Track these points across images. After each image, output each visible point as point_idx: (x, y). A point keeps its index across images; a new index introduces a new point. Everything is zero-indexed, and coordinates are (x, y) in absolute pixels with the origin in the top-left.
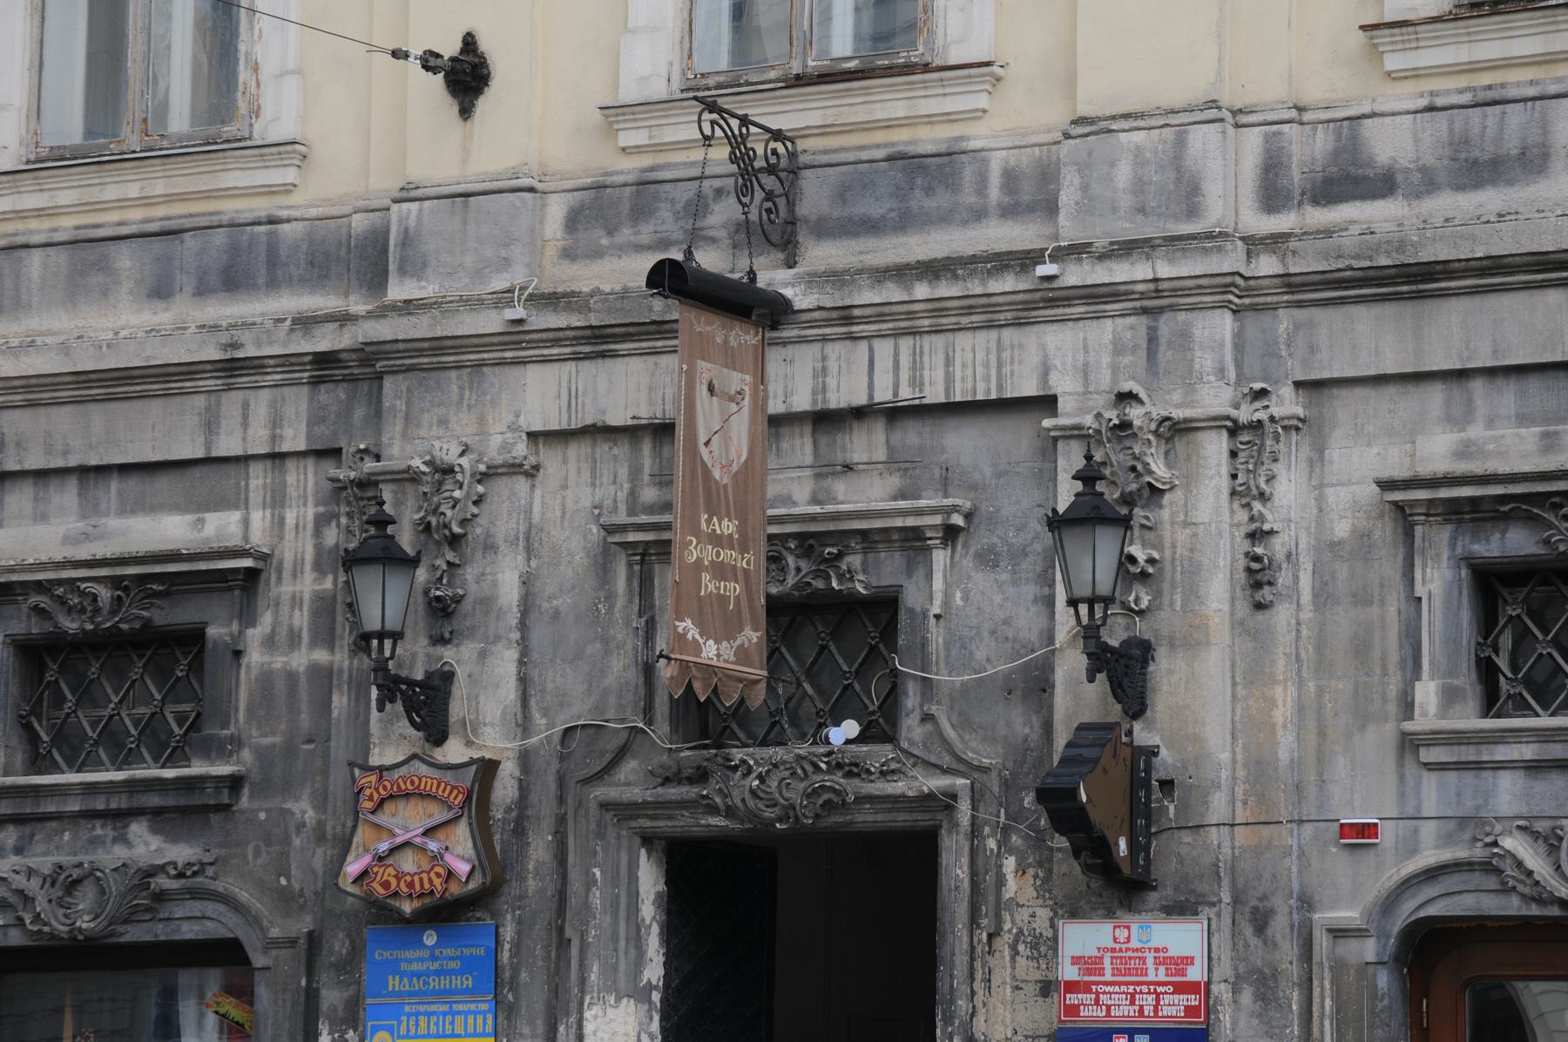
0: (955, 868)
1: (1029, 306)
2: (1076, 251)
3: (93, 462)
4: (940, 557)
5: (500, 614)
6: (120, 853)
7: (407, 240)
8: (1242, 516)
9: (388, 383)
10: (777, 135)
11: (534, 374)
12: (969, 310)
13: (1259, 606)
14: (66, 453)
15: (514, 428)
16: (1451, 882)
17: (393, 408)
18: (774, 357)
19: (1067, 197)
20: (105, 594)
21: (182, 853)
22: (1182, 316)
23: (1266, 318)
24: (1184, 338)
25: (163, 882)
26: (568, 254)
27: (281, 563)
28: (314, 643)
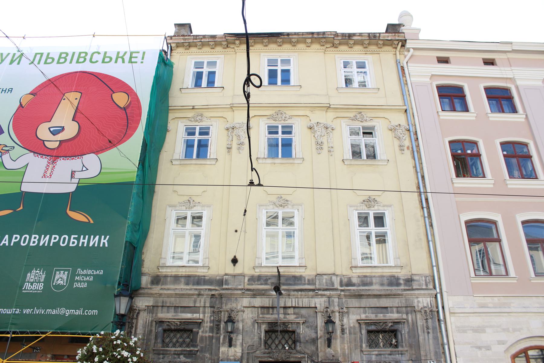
2: (319, 290)
3: (177, 305)
4: (301, 326)
5: (240, 330)
6: (179, 359)
8: (340, 323)
9: (223, 299)
12: (305, 296)
13: (343, 334)
14: (173, 304)
17: (224, 302)
19: (317, 283)
22: (333, 298)
23: (342, 299)
24: (333, 301)
26: (248, 284)
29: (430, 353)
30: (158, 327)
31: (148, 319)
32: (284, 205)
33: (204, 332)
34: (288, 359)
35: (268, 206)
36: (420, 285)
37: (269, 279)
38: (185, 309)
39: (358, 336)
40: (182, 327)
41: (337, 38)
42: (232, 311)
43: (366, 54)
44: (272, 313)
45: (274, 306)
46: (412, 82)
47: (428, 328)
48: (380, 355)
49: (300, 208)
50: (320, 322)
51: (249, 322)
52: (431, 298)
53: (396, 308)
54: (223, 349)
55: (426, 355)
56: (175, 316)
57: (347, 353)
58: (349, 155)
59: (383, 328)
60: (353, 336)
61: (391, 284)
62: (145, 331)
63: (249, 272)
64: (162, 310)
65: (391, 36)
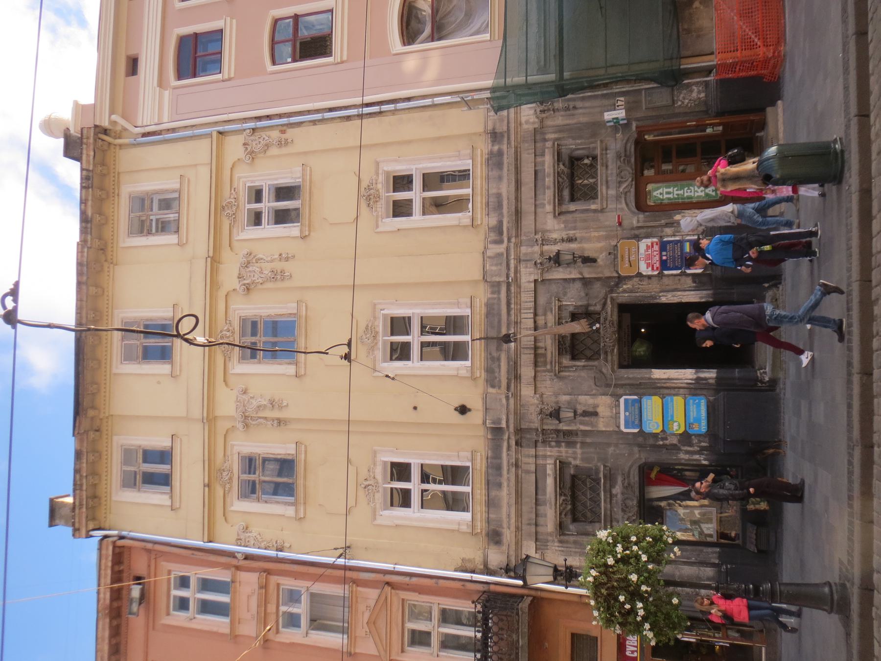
4: (564, 303)
7: (493, 423)
8: (559, 244)
9: (522, 427)
11: (523, 393)
12: (517, 297)
13: (576, 239)
14: (532, 508)
15: (533, 397)
16: (628, 201)
19: (497, 279)
20: (563, 498)
21: (620, 479)
22: (521, 255)
24: (526, 254)
25: (626, 484)
26: (500, 387)
27: (558, 456)
28: (576, 448)
29: (605, 106)
30: (569, 531)
31: (557, 548)
32: (374, 332)
33: (576, 457)
34: (615, 323)
35: (375, 357)
36: (501, 120)
37: (490, 354)
38: (538, 488)
39: (578, 216)
40: (568, 492)
41: (89, 243)
42: (541, 412)
43: (118, 195)
44: (544, 349)
45: (533, 346)
46: (170, 121)
48: (607, 182)
49: (379, 307)
50: (559, 274)
51: (558, 385)
53: (537, 157)
54: (602, 425)
56: (550, 503)
58: (291, 230)
59: (567, 177)
61: (499, 165)
62: (575, 552)
64: (542, 525)
65: (87, 150)
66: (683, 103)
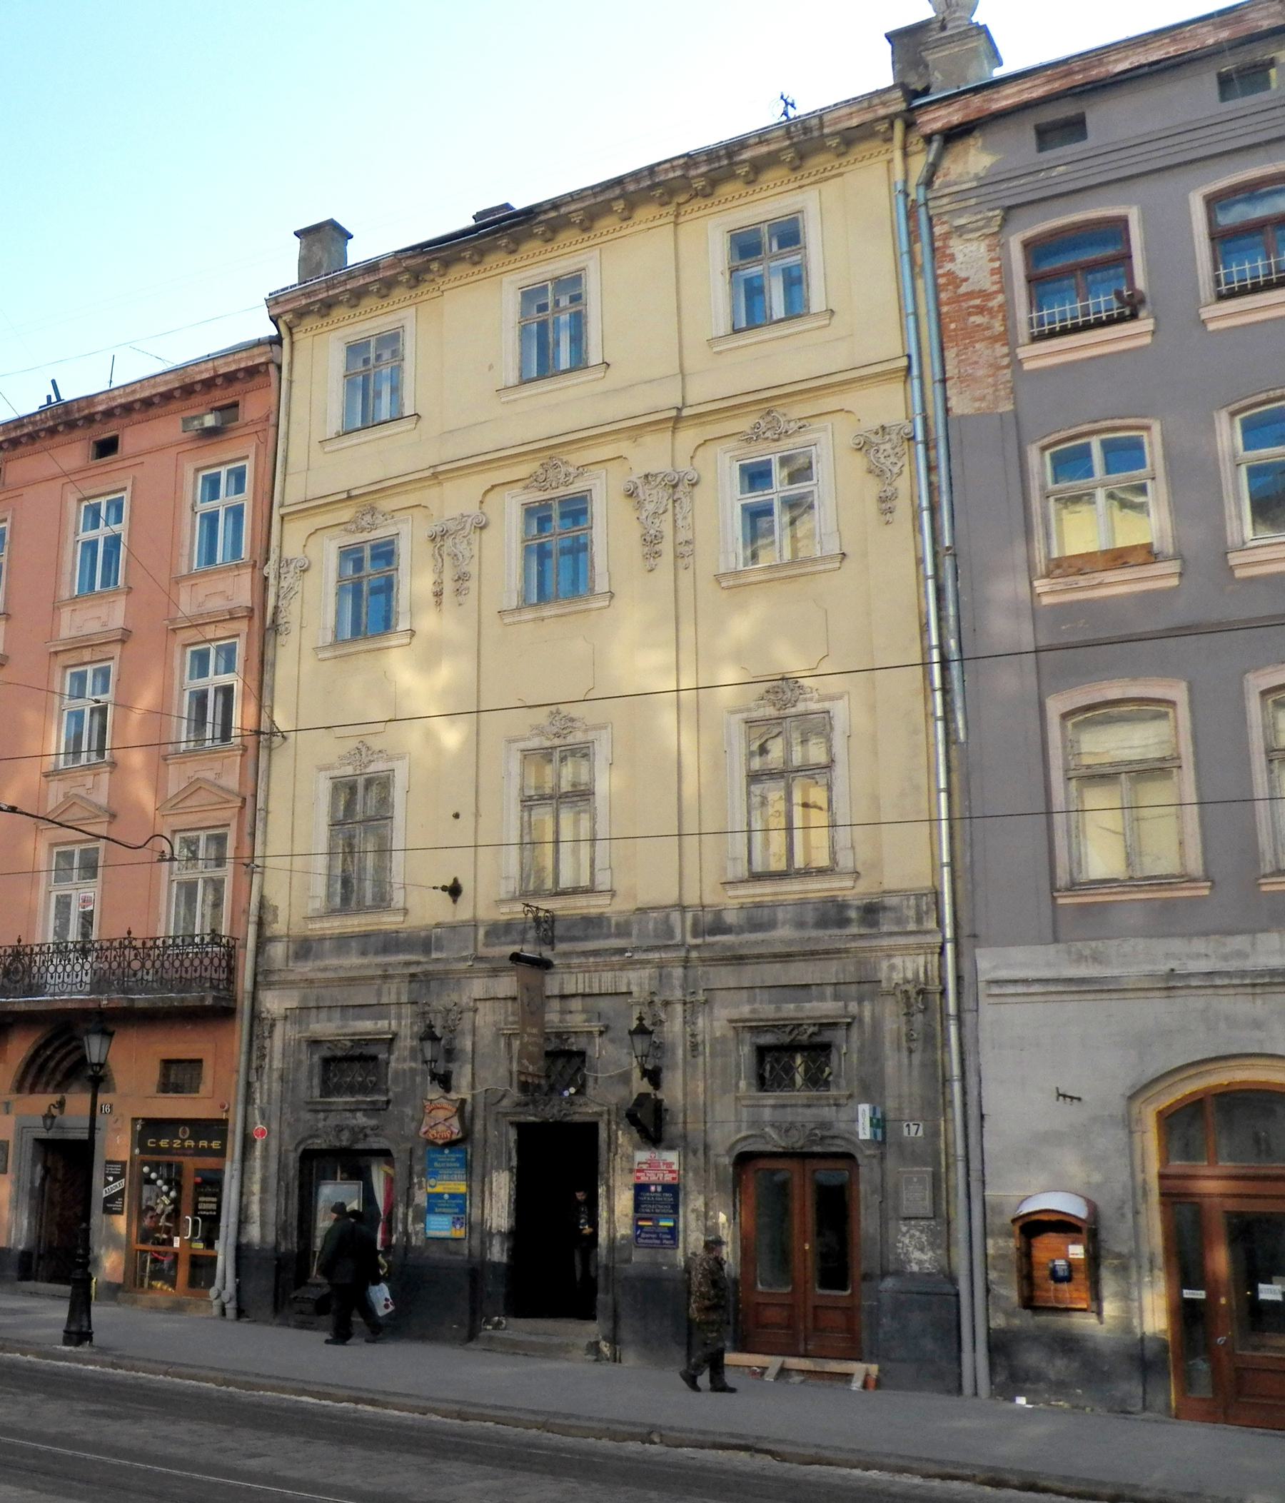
0: (603, 1135)
1: (624, 965)
10: (547, 911)
11: (476, 981)
16: (751, 1141)
18: (548, 979)
19: (635, 932)
21: (373, 1122)
24: (670, 975)
26: (486, 945)
33: (399, 1062)
34: (568, 1118)
36: (899, 921)
40: (357, 1052)
47: (910, 1038)
48: (784, 1106)
51: (486, 1034)
52: (929, 957)
55: (900, 1109)
56: (342, 1027)
57: (701, 1102)
60: (719, 1061)
61: (822, 923)
63: (487, 913)
66: (904, 1235)
